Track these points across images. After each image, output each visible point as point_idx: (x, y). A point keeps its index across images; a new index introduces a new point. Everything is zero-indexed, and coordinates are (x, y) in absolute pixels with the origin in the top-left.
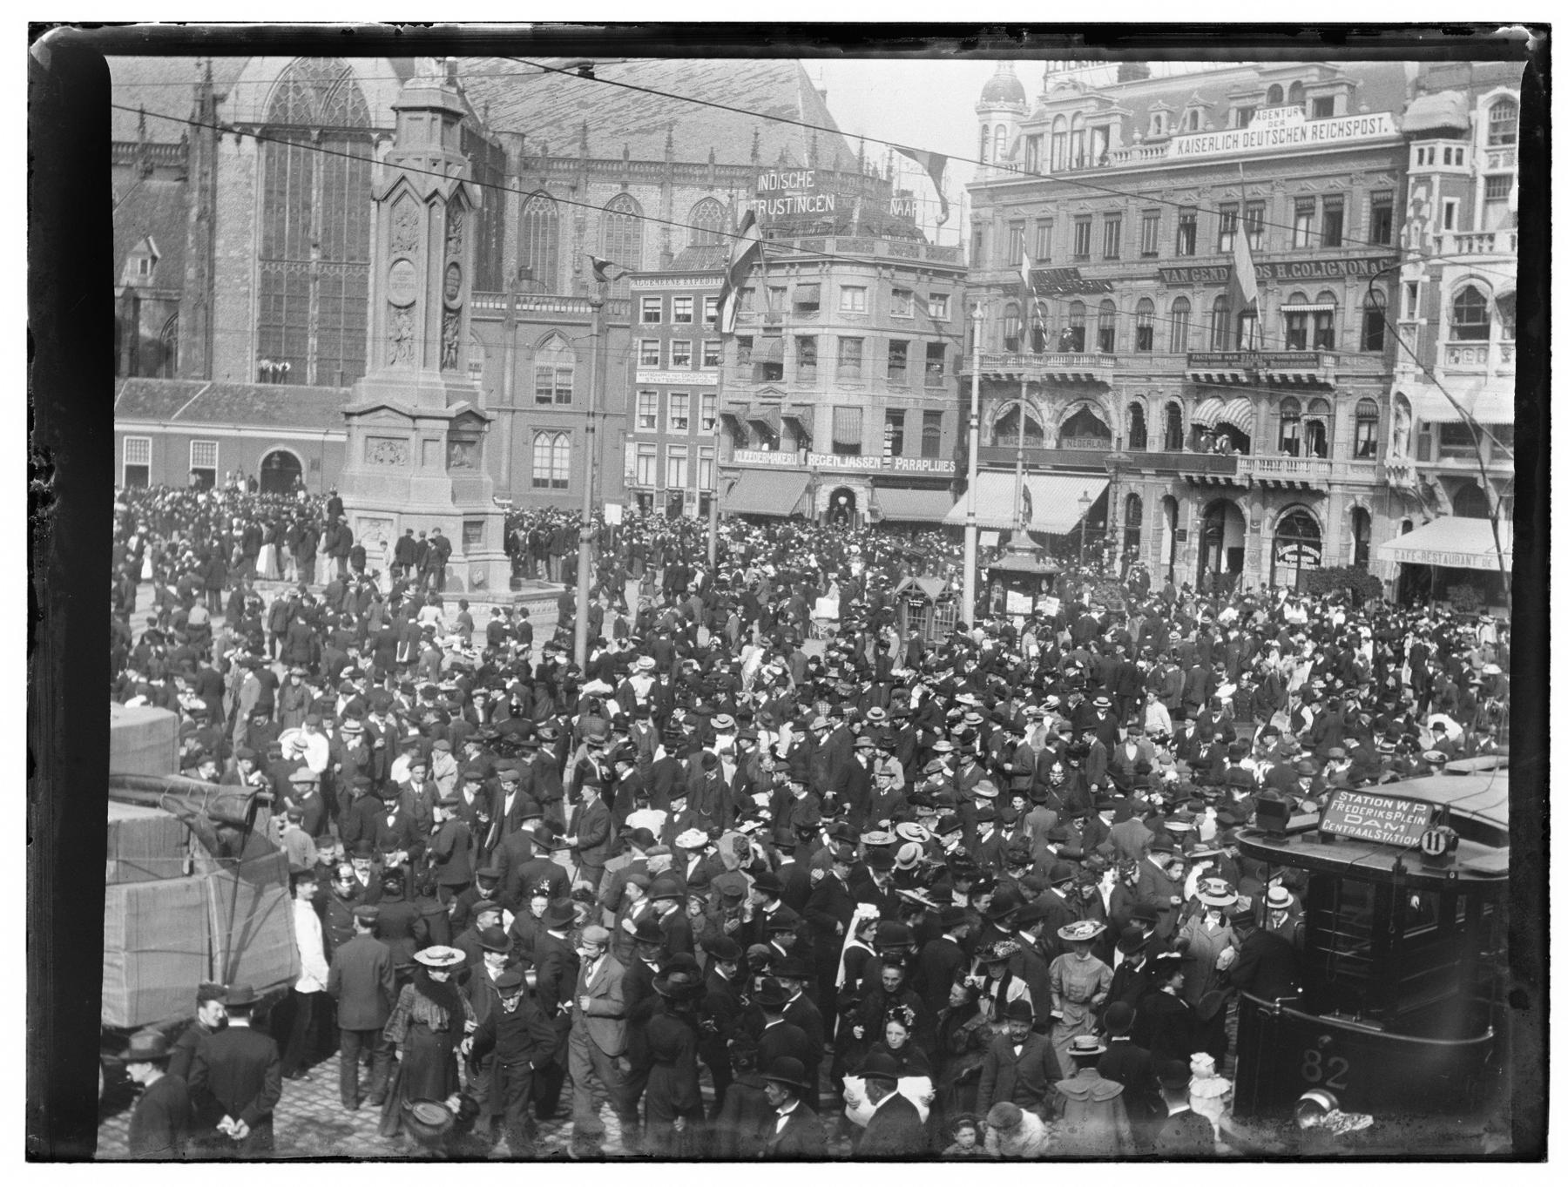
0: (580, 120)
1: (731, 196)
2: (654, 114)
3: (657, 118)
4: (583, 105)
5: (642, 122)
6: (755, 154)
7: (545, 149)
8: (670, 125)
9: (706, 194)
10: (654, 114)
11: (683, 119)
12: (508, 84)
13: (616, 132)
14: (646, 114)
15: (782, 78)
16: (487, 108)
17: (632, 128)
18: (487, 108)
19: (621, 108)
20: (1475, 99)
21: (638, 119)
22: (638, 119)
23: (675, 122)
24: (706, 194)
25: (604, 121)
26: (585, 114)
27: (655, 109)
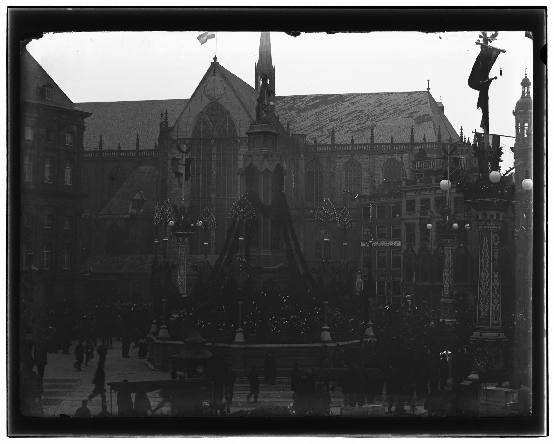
2: (365, 122)
3: (367, 124)
4: (332, 120)
5: (359, 126)
6: (412, 138)
7: (315, 141)
9: (390, 157)
10: (365, 122)
11: (378, 124)
13: (348, 131)
14: (362, 122)
15: (422, 103)
16: (288, 125)
17: (355, 129)
18: (288, 125)
20: (411, 141)
22: (357, 125)
23: (375, 125)
24: (390, 157)
25: (342, 127)
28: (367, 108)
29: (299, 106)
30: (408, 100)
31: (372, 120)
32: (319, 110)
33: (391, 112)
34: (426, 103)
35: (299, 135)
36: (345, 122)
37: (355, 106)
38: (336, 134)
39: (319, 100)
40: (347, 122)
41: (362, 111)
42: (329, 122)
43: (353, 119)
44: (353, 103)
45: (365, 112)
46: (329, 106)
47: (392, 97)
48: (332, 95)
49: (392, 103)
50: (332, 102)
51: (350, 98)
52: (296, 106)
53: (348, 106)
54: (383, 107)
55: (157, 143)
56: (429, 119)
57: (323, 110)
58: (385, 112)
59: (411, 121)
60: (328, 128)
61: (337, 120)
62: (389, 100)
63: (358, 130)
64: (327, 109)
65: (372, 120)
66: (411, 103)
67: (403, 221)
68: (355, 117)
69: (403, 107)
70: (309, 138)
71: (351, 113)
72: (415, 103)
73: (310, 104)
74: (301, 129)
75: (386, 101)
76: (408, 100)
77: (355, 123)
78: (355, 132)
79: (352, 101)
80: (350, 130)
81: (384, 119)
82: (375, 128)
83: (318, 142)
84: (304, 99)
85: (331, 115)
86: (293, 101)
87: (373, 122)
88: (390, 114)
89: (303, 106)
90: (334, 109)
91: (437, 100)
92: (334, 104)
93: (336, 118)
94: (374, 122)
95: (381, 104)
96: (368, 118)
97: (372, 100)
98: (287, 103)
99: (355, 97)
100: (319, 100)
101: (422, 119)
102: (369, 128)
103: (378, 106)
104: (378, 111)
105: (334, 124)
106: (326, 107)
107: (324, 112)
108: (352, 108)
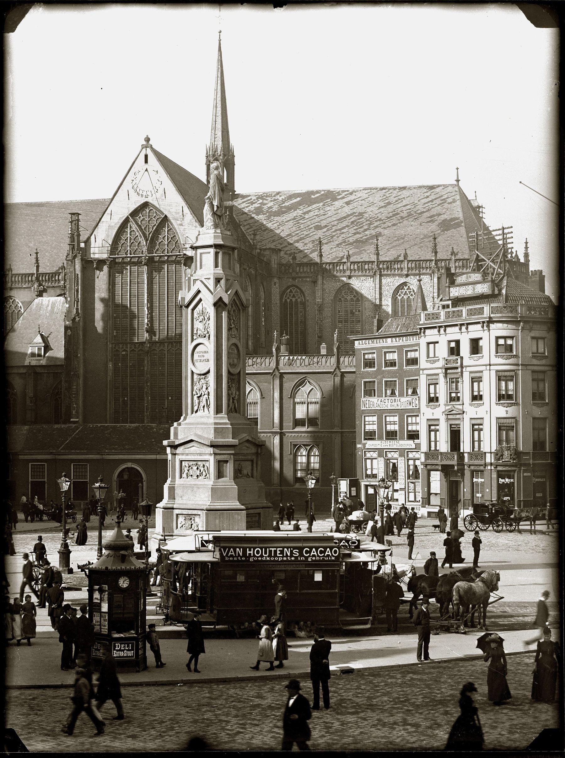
0: (316, 237)
1: (420, 281)
2: (366, 230)
4: (318, 228)
5: (358, 236)
7: (294, 258)
8: (377, 236)
10: (366, 230)
12: (269, 217)
13: (341, 244)
14: (362, 230)
15: (449, 200)
16: (255, 235)
19: (344, 228)
21: (355, 234)
22: (355, 234)
23: (380, 233)
25: (332, 237)
26: (320, 234)
27: (366, 227)
28: (369, 209)
29: (271, 207)
30: (428, 197)
31: (376, 227)
32: (299, 212)
33: (402, 214)
34: (454, 201)
35: (270, 249)
36: (336, 230)
37: (351, 206)
38: (325, 248)
39: (298, 199)
40: (340, 230)
41: (361, 214)
42: (313, 230)
43: (348, 226)
44: (348, 203)
45: (366, 215)
46: (314, 206)
47: (405, 193)
48: (318, 192)
49: (404, 203)
50: (316, 201)
51: (343, 195)
52: (265, 207)
53: (342, 207)
54: (390, 208)
55: (65, 262)
56: (458, 225)
57: (304, 214)
58: (394, 215)
59: (433, 227)
60: (312, 239)
61: (326, 226)
62: (400, 197)
63: (357, 241)
64: (310, 211)
65: (376, 227)
66: (432, 201)
67: (421, 372)
68: (352, 222)
69: (420, 208)
70: (285, 254)
71: (345, 217)
72: (438, 202)
73: (286, 204)
74: (274, 241)
75: (396, 199)
76: (428, 197)
77: (352, 231)
78: (351, 244)
79: (346, 200)
80: (345, 242)
81: (394, 225)
82: (380, 238)
83: (298, 259)
84: (278, 197)
85: (317, 219)
86: (261, 201)
87: (377, 230)
88: (402, 218)
89: (275, 208)
90: (322, 212)
91: (470, 196)
92: (321, 204)
93: (323, 224)
94: (379, 230)
95: (389, 203)
96: (370, 224)
97: (377, 198)
98: (252, 203)
99: (351, 194)
100: (298, 199)
101: (447, 225)
102: (372, 237)
103: (385, 206)
104: (386, 212)
105: (320, 234)
106: (310, 208)
107: (307, 216)
108: (347, 210)
